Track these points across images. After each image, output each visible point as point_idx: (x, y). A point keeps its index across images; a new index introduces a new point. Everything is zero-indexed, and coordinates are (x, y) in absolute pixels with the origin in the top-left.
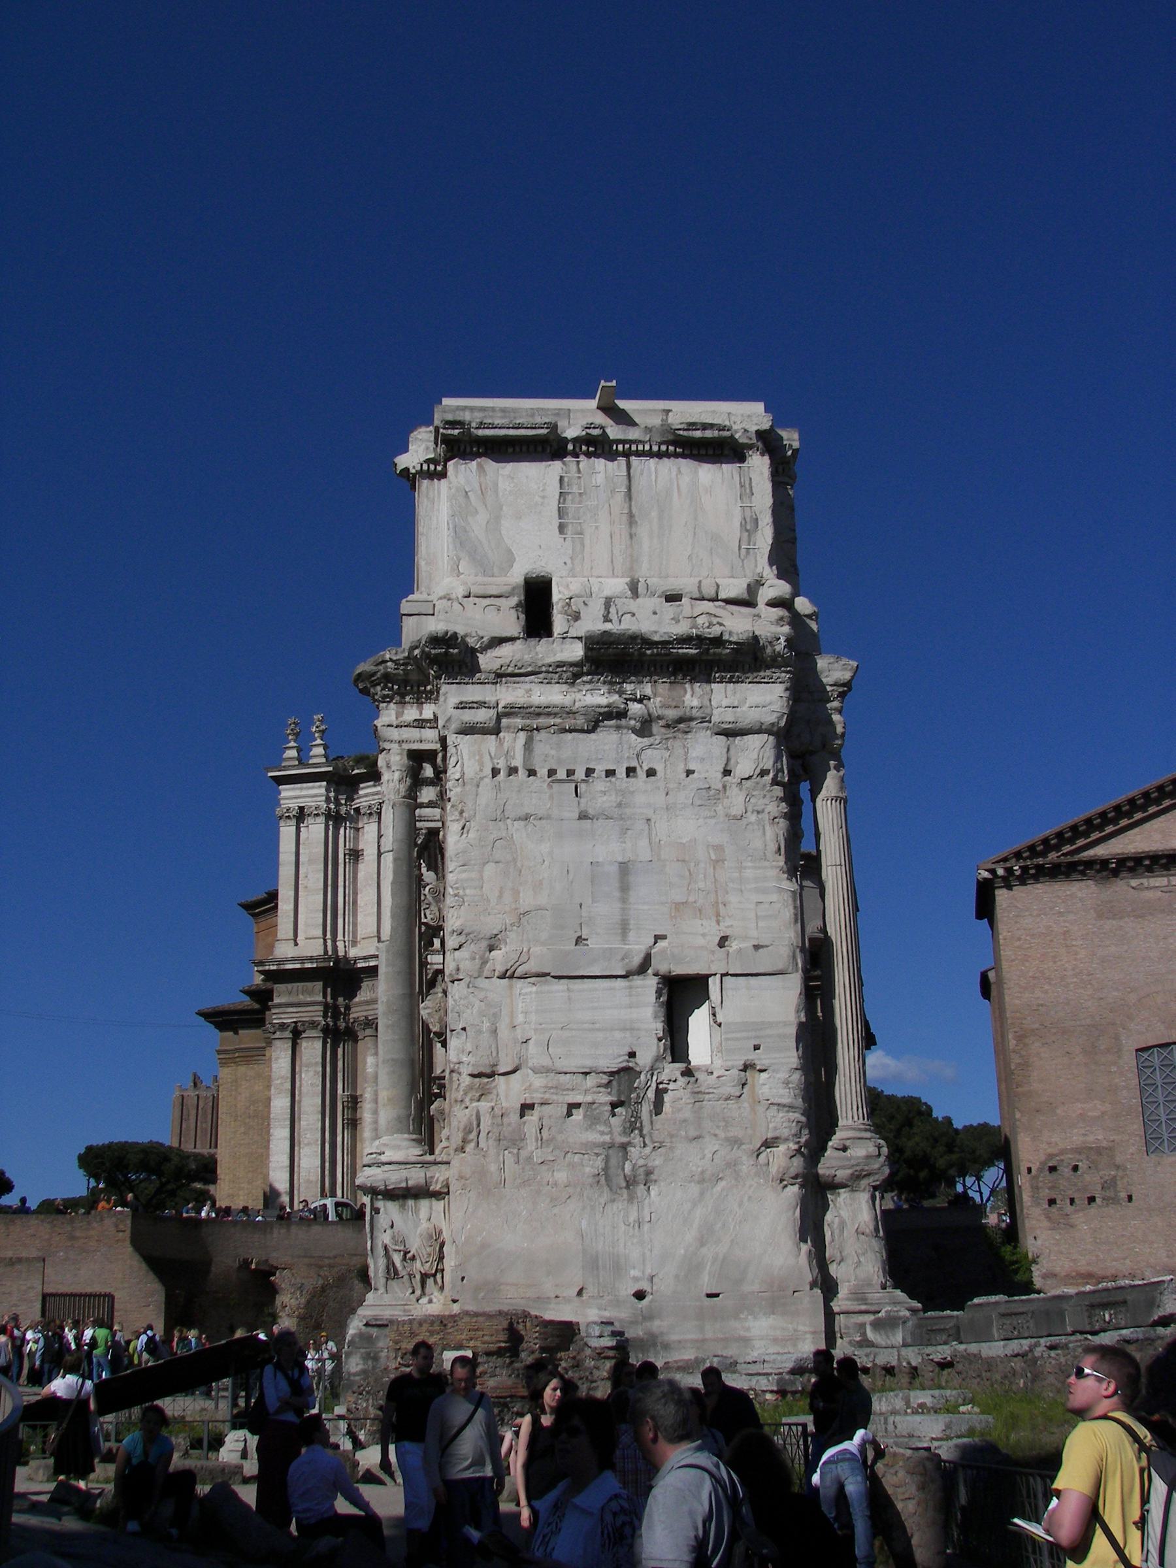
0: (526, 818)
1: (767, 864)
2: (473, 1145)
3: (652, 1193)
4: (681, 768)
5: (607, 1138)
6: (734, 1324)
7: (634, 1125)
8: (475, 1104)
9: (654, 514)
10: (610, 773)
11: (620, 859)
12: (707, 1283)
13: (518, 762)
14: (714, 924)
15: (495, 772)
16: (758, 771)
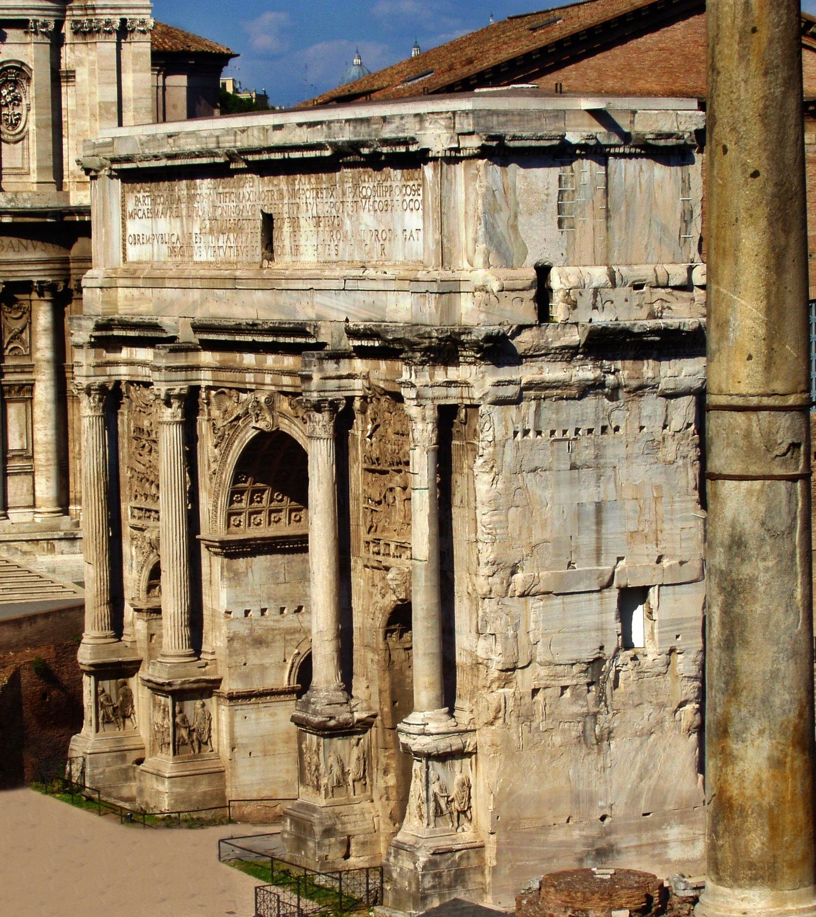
0: (534, 470)
1: (689, 498)
2: (501, 721)
3: (612, 746)
4: (636, 425)
5: (585, 710)
6: (658, 833)
7: (601, 698)
8: (501, 691)
9: (623, 209)
10: (590, 431)
11: (596, 500)
12: (643, 807)
13: (530, 426)
14: (655, 546)
15: (516, 433)
16: (685, 425)
